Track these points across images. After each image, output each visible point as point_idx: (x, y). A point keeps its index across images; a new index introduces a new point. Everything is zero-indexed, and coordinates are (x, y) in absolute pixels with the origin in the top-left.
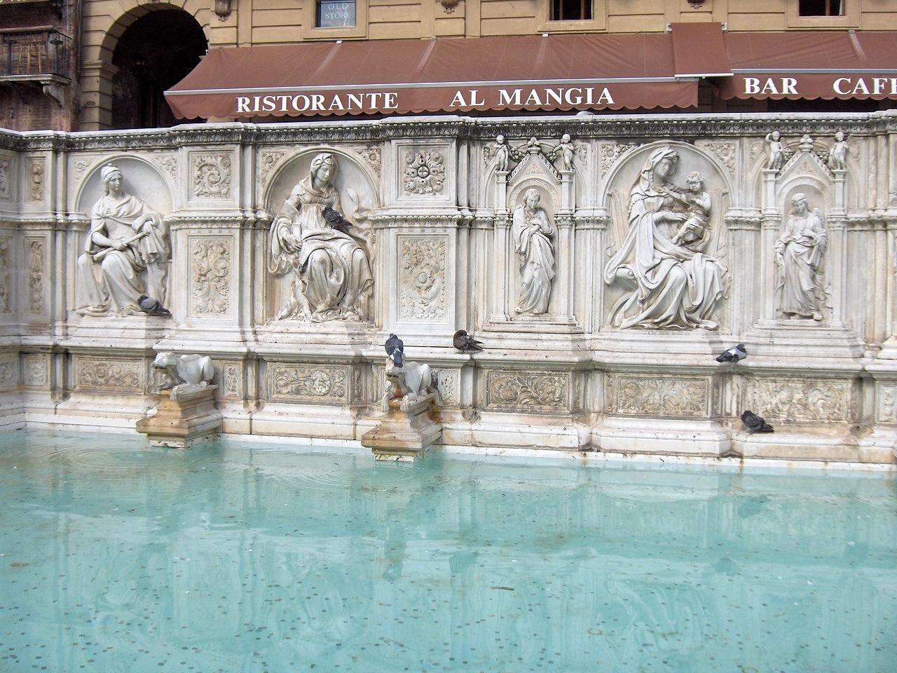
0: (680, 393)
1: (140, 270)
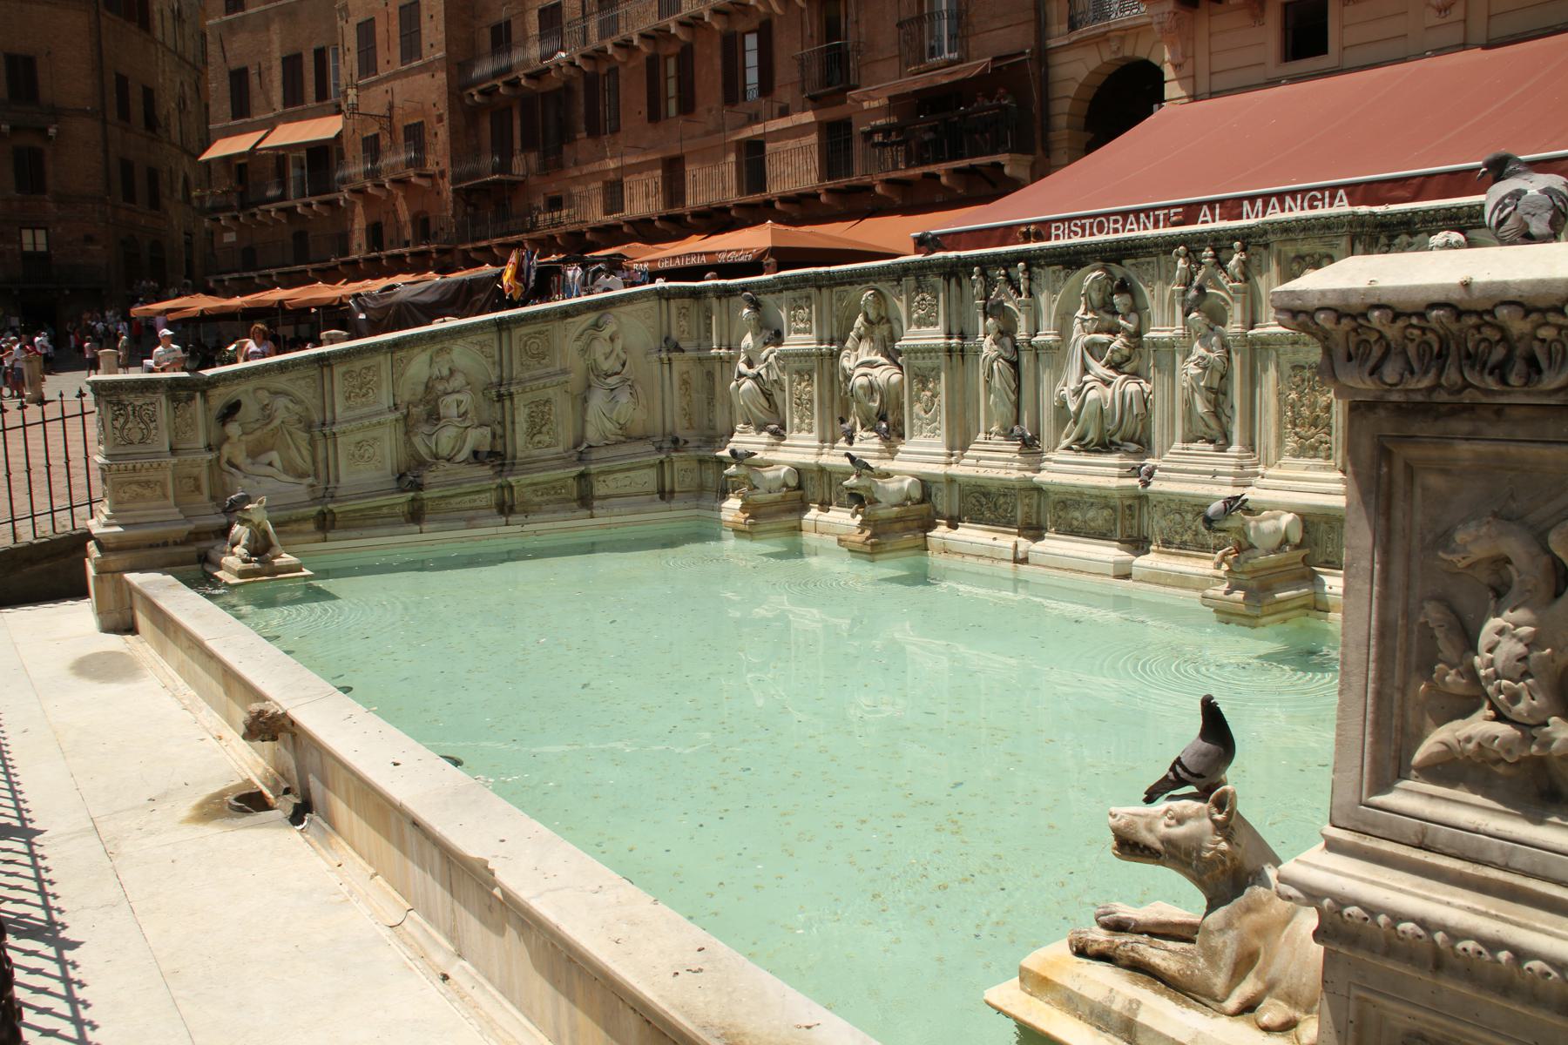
0: (1097, 517)
1: (768, 396)
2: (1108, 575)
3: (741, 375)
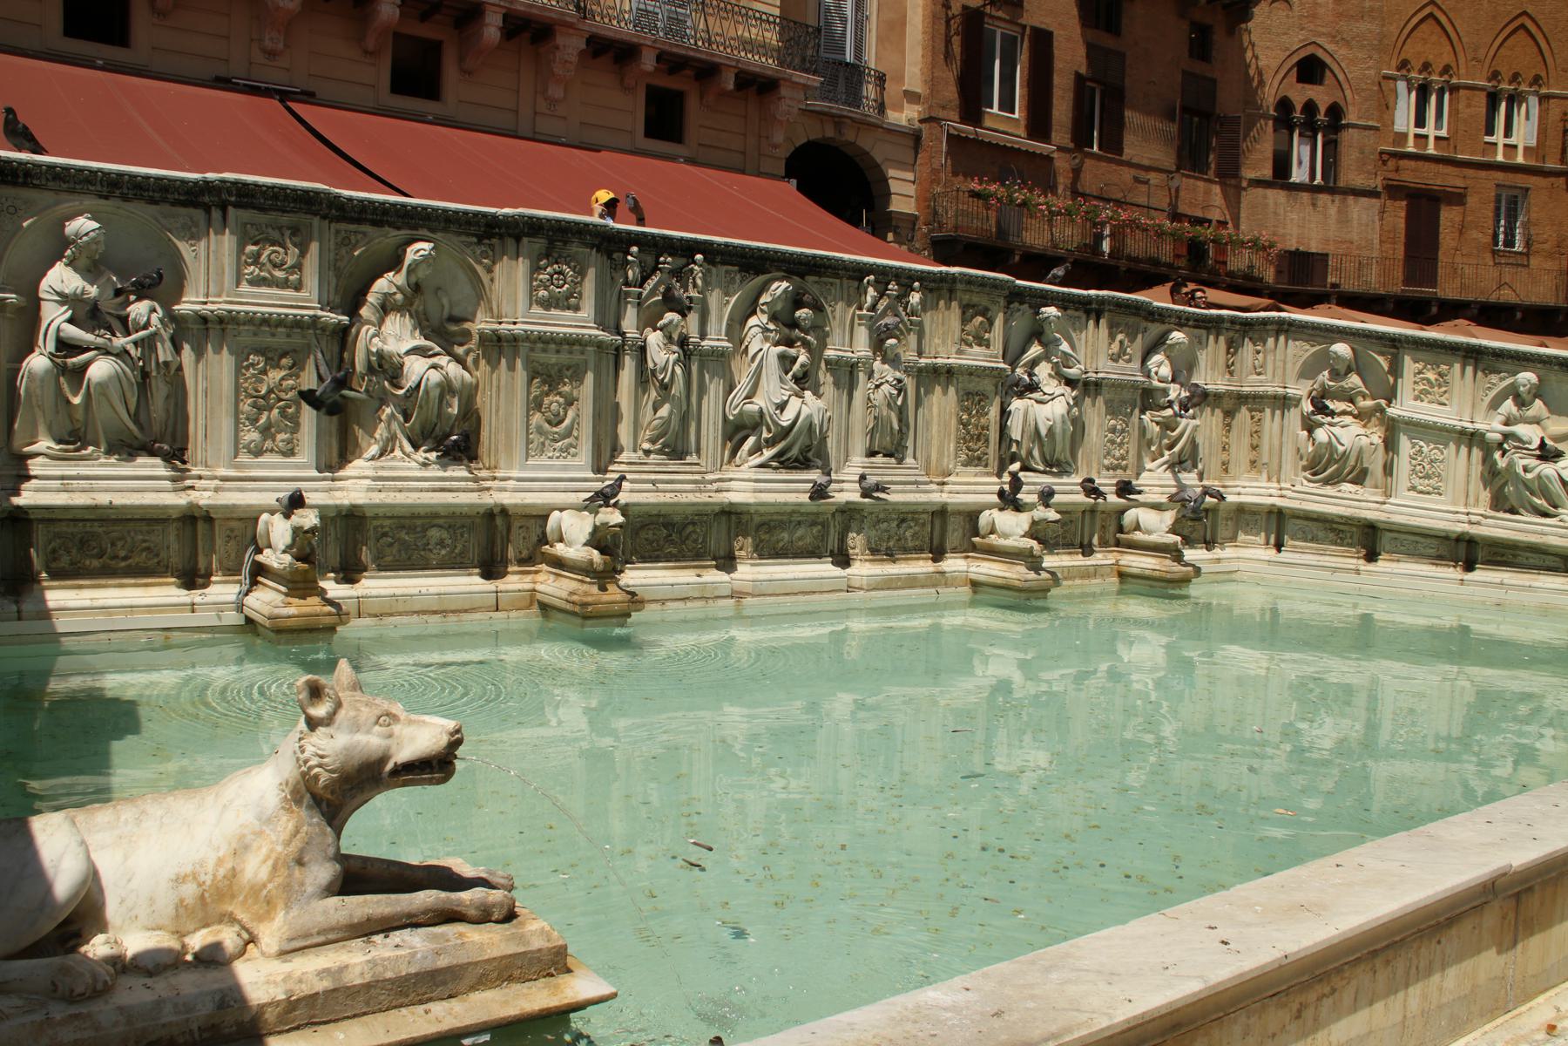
0: (804, 535)
2: (841, 590)
3: (66, 347)
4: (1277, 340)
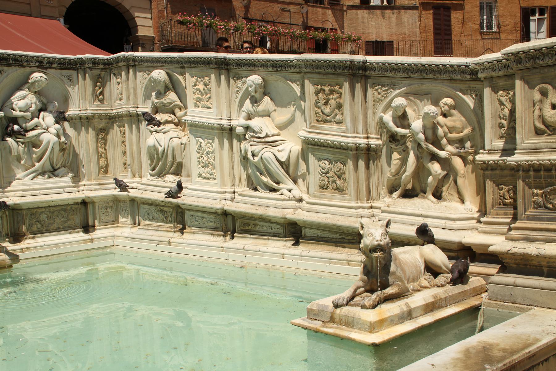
4: (128, 73)
